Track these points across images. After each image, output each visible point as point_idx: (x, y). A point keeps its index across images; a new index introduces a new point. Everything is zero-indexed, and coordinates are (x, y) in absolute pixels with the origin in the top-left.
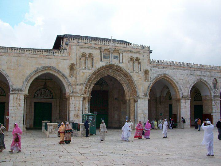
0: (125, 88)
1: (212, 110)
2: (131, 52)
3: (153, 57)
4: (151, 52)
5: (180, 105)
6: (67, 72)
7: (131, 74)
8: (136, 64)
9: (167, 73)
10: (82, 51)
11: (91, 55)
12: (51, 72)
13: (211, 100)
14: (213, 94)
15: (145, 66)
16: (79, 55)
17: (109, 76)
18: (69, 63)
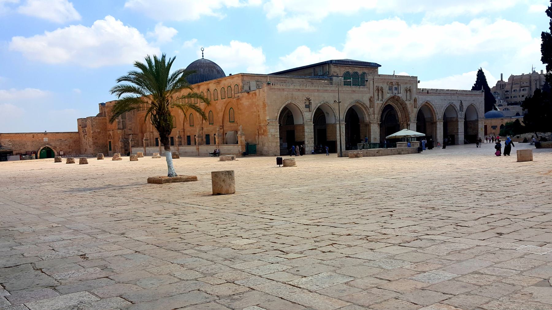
0: (399, 114)
1: (458, 129)
2: (406, 83)
3: (420, 86)
4: (419, 82)
5: (436, 127)
6: (368, 104)
7: (406, 102)
8: (409, 92)
9: (428, 99)
10: (376, 85)
11: (382, 89)
12: (357, 104)
13: (457, 121)
14: (459, 116)
15: (414, 96)
16: (375, 88)
17: (389, 105)
18: (368, 96)
